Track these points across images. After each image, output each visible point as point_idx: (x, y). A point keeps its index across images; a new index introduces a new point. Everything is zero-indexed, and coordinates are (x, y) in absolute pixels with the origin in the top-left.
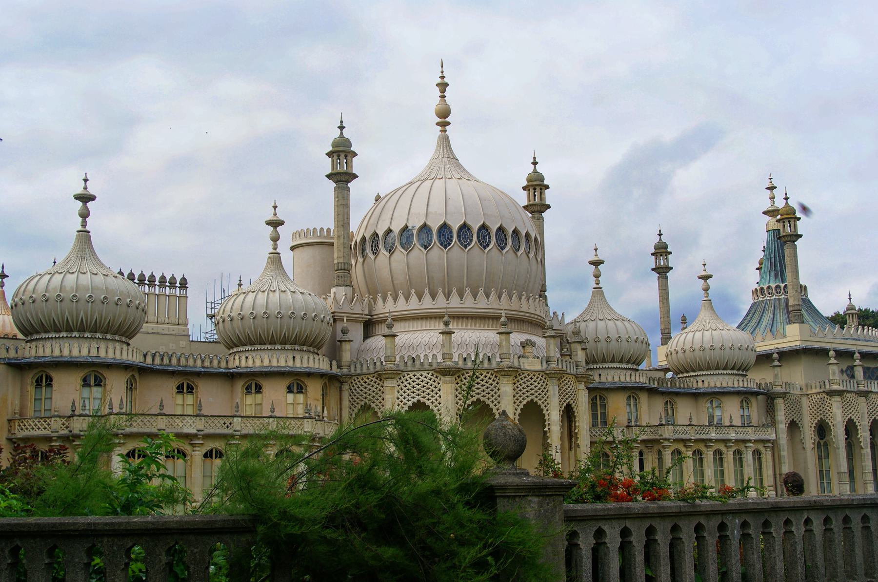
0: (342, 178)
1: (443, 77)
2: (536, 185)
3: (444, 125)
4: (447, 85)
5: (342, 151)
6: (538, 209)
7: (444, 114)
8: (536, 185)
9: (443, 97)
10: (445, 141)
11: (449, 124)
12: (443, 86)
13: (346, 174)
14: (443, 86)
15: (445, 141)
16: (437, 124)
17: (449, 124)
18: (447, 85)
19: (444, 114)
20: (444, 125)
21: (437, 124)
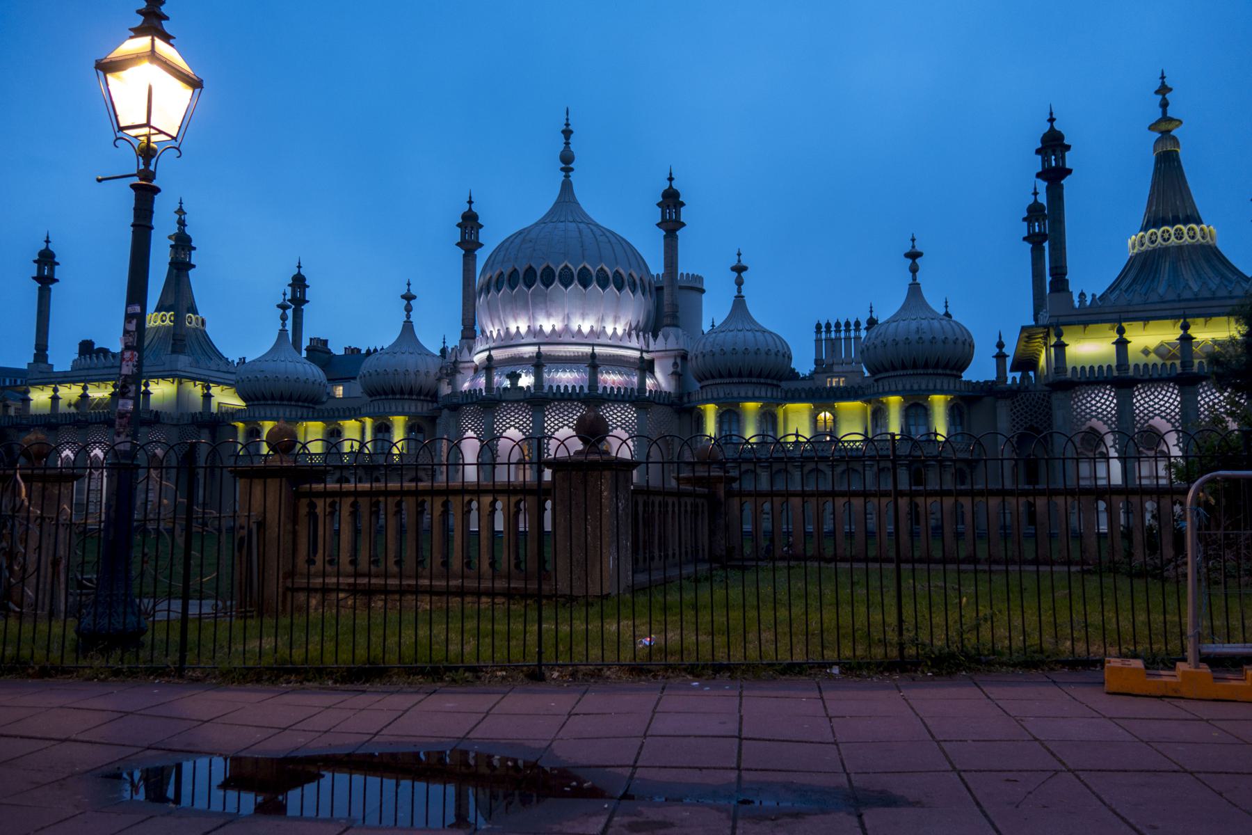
0: (469, 245)
1: (567, 125)
2: (671, 200)
3: (567, 170)
4: (571, 132)
5: (470, 222)
6: (671, 226)
7: (567, 159)
8: (671, 200)
9: (567, 144)
10: (567, 187)
11: (572, 170)
12: (567, 133)
13: (473, 242)
14: (567, 133)
15: (567, 187)
16: (562, 169)
17: (572, 170)
18: (571, 132)
19: (567, 159)
20: (567, 170)
21: (562, 169)
